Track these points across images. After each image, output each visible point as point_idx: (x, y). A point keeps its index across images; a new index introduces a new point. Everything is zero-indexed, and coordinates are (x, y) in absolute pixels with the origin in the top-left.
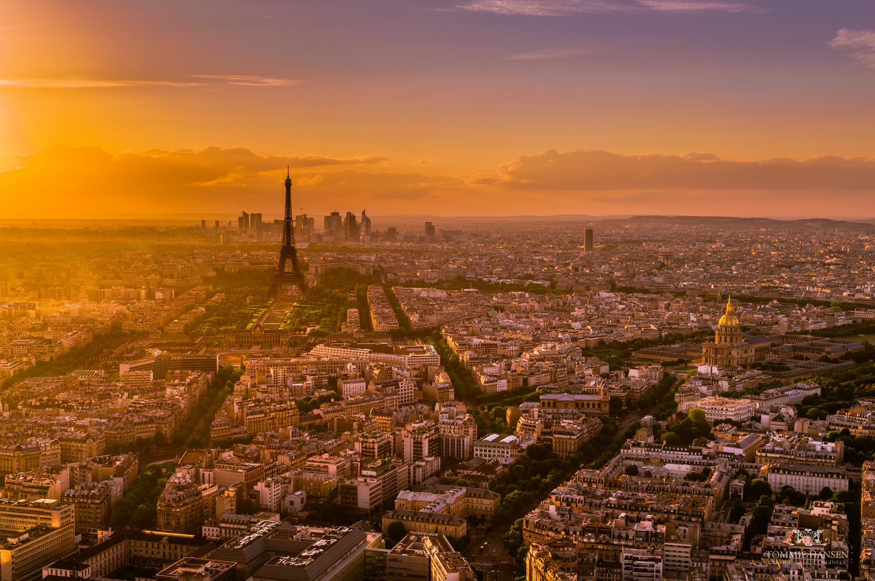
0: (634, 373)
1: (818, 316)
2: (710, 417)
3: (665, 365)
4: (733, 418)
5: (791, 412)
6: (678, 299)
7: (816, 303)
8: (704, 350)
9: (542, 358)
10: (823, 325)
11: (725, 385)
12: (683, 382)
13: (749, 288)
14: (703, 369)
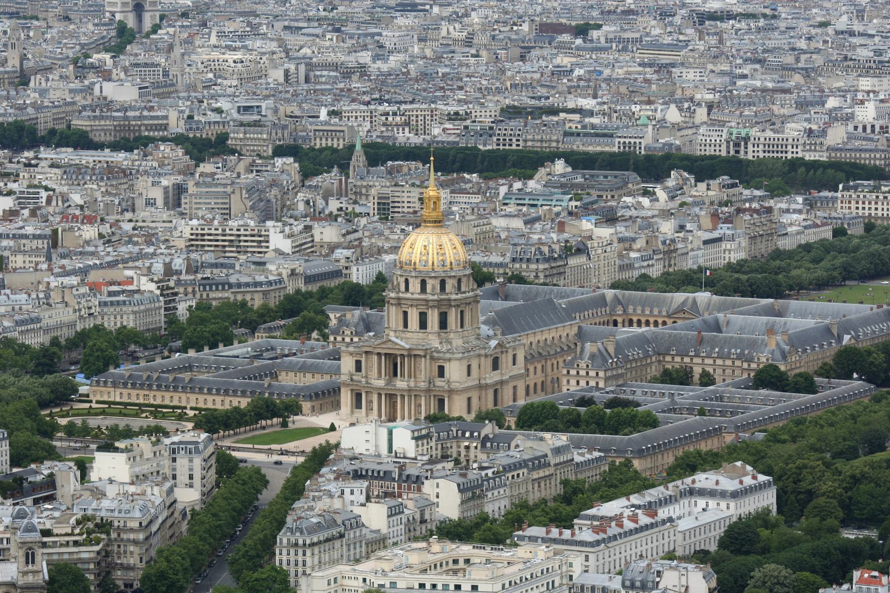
1: (715, 216)
6: (207, 167)
7: (704, 168)
8: (347, 364)
10: (735, 252)
13: (455, 117)
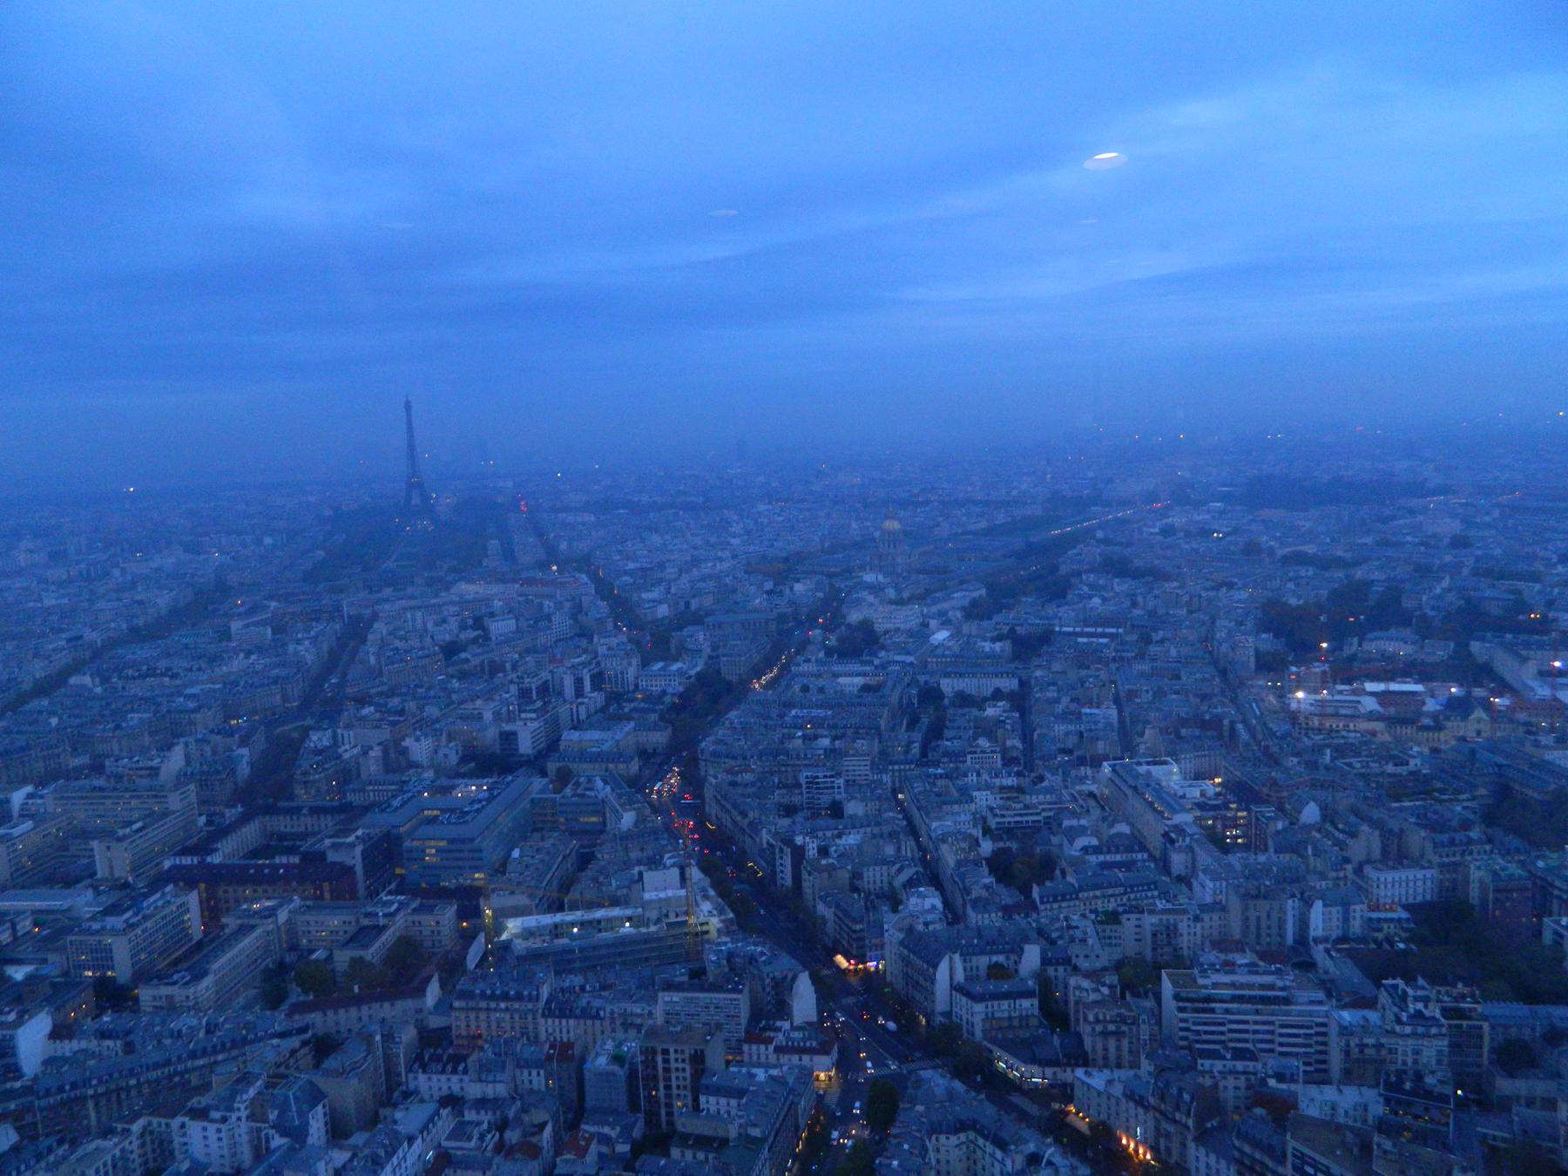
0: (798, 587)
2: (880, 626)
3: (830, 575)
4: (902, 627)
5: (959, 614)
9: (703, 579)
11: (891, 593)
12: (849, 593)
14: (869, 577)
